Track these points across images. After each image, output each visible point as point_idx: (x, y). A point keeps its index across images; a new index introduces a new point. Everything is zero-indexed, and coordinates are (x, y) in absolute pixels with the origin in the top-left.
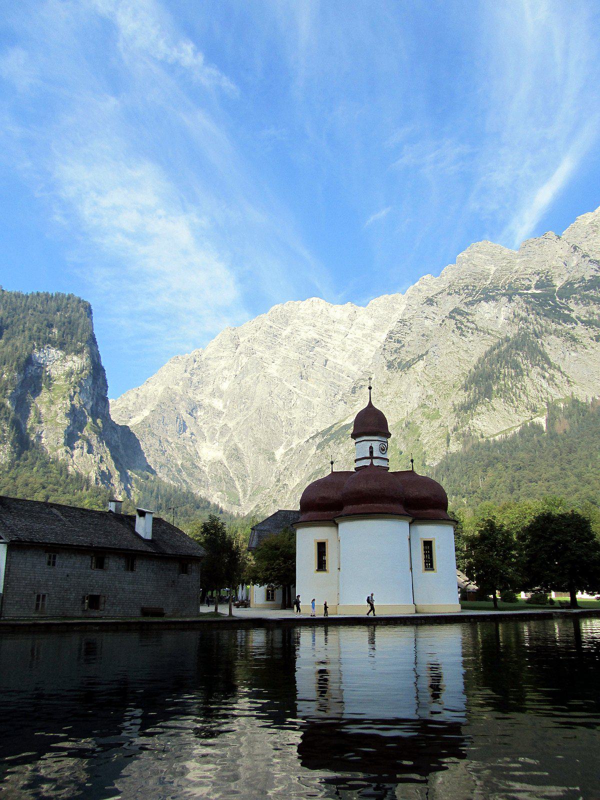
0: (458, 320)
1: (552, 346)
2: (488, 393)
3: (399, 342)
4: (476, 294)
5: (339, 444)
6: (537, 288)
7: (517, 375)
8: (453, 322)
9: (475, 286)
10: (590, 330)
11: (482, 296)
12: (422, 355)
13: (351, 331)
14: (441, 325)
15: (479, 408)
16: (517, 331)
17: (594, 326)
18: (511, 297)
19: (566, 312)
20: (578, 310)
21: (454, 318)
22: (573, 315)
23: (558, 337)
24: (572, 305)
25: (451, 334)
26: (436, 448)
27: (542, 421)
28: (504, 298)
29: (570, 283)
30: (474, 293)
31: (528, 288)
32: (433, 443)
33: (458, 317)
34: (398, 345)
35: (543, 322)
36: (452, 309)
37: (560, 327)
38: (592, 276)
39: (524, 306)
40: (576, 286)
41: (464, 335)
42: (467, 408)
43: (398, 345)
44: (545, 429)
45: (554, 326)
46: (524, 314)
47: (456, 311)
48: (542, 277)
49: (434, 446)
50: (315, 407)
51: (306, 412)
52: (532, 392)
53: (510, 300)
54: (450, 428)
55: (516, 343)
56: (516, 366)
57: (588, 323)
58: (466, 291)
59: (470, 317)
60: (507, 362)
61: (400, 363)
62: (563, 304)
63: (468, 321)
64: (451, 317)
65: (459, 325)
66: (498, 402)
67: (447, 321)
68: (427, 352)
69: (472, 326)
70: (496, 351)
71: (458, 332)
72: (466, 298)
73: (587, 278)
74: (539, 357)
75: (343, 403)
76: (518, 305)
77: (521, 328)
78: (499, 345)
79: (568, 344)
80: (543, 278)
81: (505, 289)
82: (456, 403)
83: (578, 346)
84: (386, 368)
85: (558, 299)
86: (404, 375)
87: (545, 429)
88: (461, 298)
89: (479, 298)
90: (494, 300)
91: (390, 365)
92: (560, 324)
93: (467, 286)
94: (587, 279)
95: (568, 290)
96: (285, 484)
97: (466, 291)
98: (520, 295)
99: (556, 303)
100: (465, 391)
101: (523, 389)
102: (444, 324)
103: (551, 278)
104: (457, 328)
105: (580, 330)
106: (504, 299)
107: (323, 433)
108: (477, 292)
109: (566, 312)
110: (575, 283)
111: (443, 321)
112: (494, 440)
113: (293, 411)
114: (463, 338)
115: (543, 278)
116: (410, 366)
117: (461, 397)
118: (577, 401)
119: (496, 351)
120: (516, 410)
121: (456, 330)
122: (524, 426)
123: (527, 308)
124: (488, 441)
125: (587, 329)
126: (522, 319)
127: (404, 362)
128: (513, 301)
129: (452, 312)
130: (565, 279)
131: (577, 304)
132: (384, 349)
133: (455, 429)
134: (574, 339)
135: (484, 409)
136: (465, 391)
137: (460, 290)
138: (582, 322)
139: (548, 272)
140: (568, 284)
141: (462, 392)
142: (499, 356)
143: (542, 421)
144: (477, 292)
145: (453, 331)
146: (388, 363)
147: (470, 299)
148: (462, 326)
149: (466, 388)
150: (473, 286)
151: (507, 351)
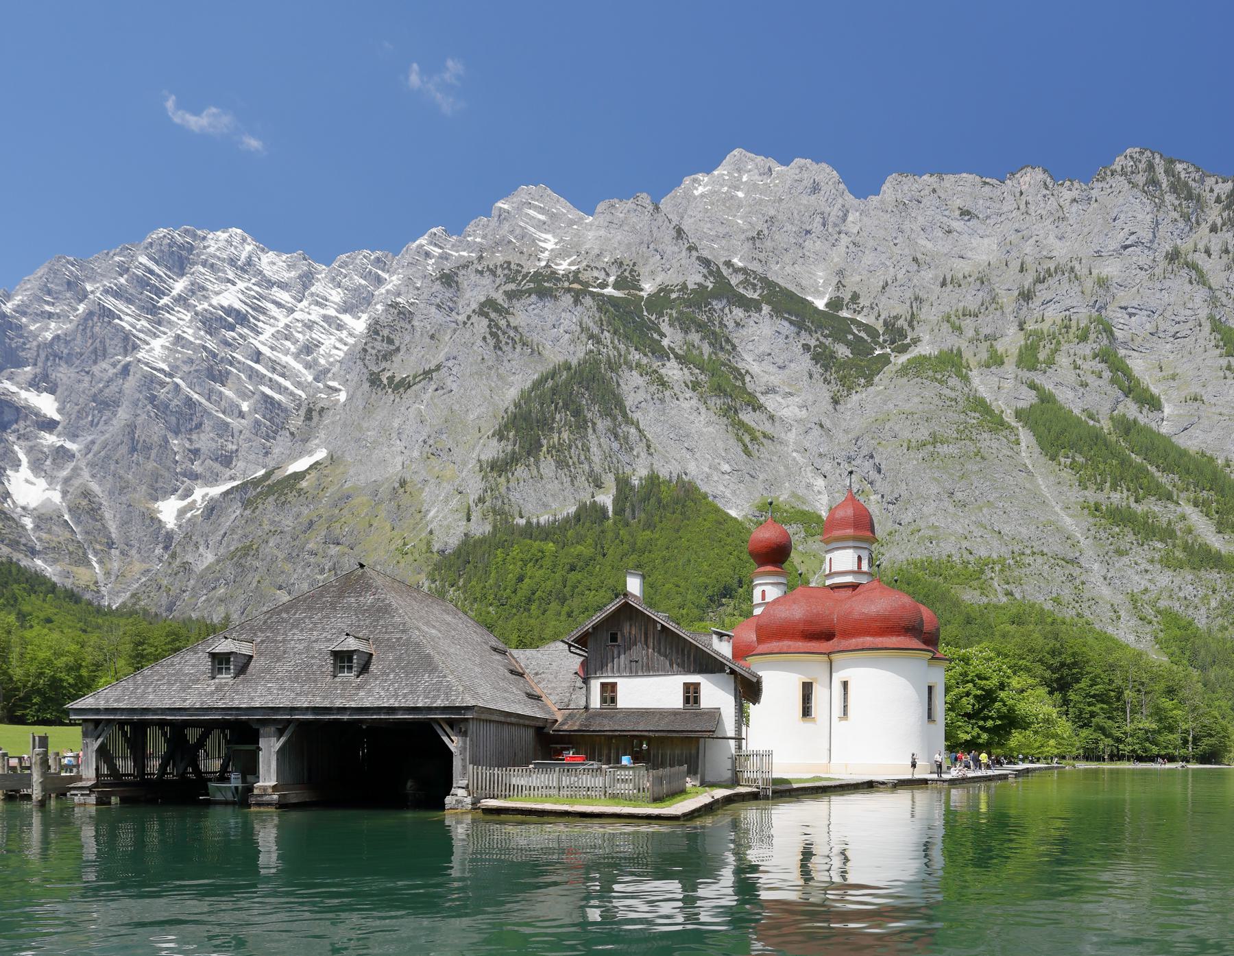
0: (493, 321)
1: (632, 386)
2: (533, 449)
3: (390, 341)
4: (522, 280)
5: (283, 504)
6: (616, 286)
7: (579, 427)
8: (485, 322)
9: (522, 267)
10: (685, 370)
11: (532, 285)
12: (430, 371)
13: (300, 305)
14: (465, 323)
15: (520, 471)
16: (582, 355)
17: (692, 366)
18: (578, 296)
19: (655, 336)
20: (671, 337)
21: (486, 315)
22: (665, 342)
23: (642, 376)
24: (665, 327)
25: (480, 342)
26: (449, 527)
27: (606, 499)
28: (568, 296)
29: (664, 290)
30: (520, 278)
31: (604, 285)
32: (445, 518)
33: (493, 315)
34: (385, 347)
35: (622, 347)
36: (483, 299)
37: (645, 361)
38: (698, 284)
39: (597, 315)
40: (674, 296)
41: (500, 349)
42: (500, 467)
43: (385, 347)
44: (610, 513)
45: (635, 356)
46: (596, 331)
47: (490, 303)
48: (625, 270)
49: (445, 523)
50: (236, 434)
51: (220, 441)
52: (597, 456)
53: (577, 301)
54: (473, 497)
55: (581, 373)
56: (577, 413)
57: (682, 360)
58: (506, 272)
59: (511, 319)
60: (566, 406)
61: (391, 379)
62: (653, 323)
63: (508, 325)
64: (481, 312)
65: (494, 330)
66: (548, 466)
67: (475, 318)
68: (438, 368)
69: (512, 334)
70: (550, 383)
71: (491, 342)
72: (505, 283)
73: (691, 286)
74: (613, 404)
75: (288, 434)
76: (587, 313)
77: (592, 351)
78: (553, 374)
79: (653, 388)
80: (627, 274)
81: (568, 280)
82: (483, 457)
83: (667, 393)
84: (366, 385)
85: (645, 313)
86: (398, 400)
87: (610, 513)
88: (498, 281)
89: (526, 287)
90: (551, 296)
91: (374, 380)
92: (645, 355)
93: (509, 263)
94: (690, 287)
95: (660, 301)
96: (187, 562)
97: (506, 272)
98: (593, 295)
99: (643, 319)
100: (500, 440)
101: (587, 449)
102: (470, 322)
103: (639, 275)
104: (491, 334)
105: (673, 371)
106: (568, 300)
107: (256, 483)
108: (525, 277)
109: (655, 336)
110: (673, 291)
111: (469, 317)
112: (538, 523)
113: (194, 437)
114: (499, 353)
115: (627, 274)
116: (410, 387)
117: (493, 450)
118: (658, 477)
119: (550, 383)
120: (572, 481)
121: (488, 336)
122: (582, 508)
123: (601, 320)
124: (529, 523)
125: (681, 369)
126: (591, 337)
127: (397, 379)
128: (582, 304)
129: (482, 305)
130: (659, 280)
131: (671, 325)
132: (365, 350)
133: (481, 500)
134: (663, 383)
135: (526, 475)
136: (500, 440)
137: (496, 268)
138: (677, 357)
139: (634, 264)
140: (660, 290)
141: (494, 442)
142: (554, 391)
143: (606, 499)
144: (525, 277)
145: (484, 338)
146: (371, 375)
147: (512, 286)
148: (499, 332)
149: (500, 435)
150: (518, 265)
151: (567, 383)
